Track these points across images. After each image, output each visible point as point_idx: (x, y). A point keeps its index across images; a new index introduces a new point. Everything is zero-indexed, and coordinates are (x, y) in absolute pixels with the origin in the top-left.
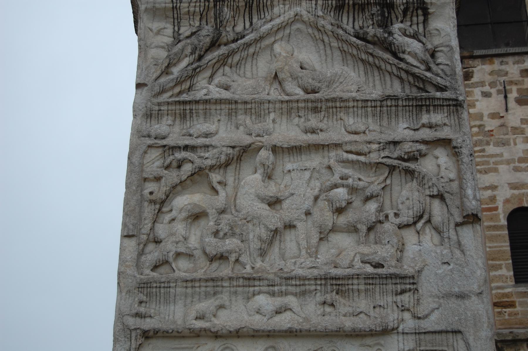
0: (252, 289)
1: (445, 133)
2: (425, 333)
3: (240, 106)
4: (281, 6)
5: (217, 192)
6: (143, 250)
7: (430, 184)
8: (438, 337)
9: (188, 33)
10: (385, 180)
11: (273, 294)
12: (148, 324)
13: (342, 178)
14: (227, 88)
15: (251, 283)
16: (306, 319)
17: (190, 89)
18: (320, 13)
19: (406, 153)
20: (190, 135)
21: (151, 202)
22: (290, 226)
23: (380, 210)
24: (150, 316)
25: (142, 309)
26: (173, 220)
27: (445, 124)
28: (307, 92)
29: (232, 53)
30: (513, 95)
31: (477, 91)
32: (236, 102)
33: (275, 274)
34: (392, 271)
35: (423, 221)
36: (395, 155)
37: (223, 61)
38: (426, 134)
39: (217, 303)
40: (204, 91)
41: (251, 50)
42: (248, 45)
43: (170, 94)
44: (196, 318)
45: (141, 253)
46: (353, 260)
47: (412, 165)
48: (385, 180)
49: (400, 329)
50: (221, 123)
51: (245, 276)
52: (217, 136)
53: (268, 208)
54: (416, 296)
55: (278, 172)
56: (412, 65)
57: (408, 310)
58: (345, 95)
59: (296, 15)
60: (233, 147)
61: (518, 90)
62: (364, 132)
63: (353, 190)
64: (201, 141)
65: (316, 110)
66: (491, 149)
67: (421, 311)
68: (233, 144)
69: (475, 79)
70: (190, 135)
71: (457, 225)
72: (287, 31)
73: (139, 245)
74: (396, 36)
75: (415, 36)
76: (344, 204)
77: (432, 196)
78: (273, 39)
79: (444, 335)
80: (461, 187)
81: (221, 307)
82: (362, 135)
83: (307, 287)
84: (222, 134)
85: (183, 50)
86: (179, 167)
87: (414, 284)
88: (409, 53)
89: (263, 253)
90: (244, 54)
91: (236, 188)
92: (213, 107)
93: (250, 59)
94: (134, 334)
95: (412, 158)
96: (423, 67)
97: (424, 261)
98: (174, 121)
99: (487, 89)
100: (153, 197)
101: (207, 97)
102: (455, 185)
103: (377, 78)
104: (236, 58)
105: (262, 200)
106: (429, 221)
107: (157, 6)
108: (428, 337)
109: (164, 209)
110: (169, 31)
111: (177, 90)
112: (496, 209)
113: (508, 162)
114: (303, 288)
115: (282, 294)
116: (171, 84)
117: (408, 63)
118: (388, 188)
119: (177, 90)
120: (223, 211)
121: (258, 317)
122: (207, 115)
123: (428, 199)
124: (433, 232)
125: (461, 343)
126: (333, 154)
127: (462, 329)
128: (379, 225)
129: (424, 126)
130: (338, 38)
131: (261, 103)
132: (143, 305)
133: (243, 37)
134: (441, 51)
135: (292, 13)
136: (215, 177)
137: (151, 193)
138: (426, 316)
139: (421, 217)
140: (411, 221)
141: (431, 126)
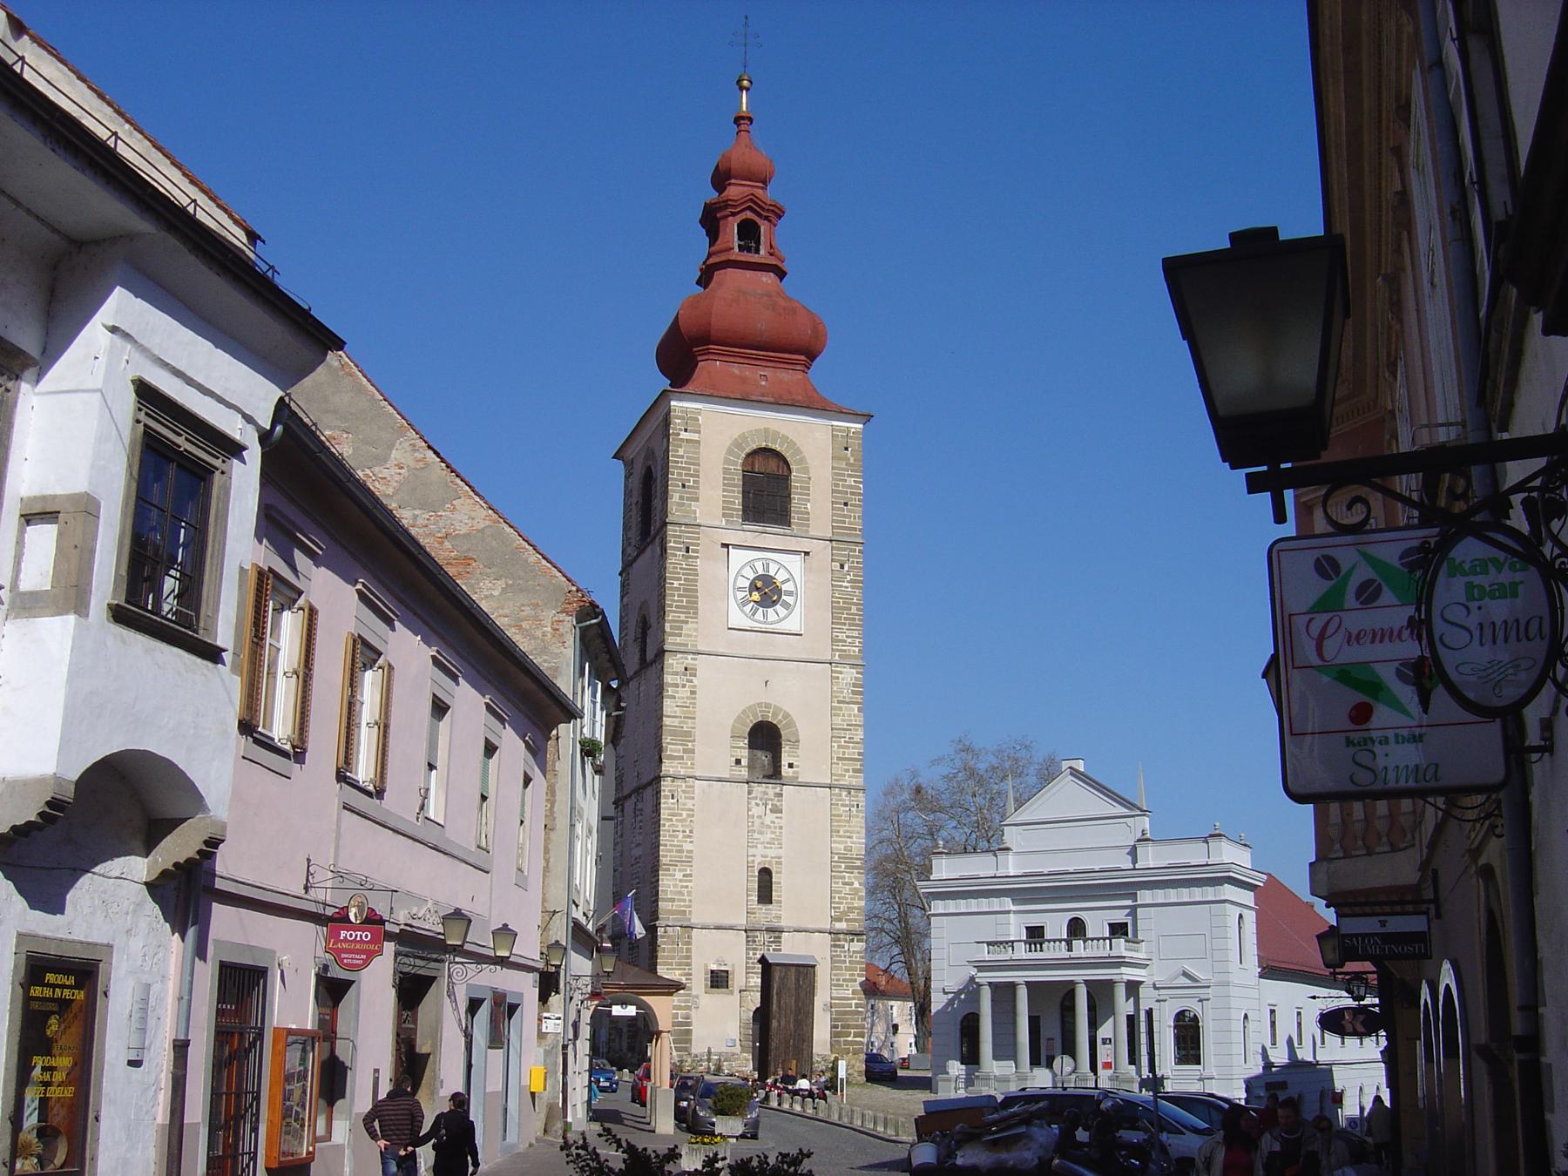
30: (769, 807)
31: (753, 802)
61: (772, 805)
66: (756, 835)
69: (753, 795)
99: (758, 801)
112: (754, 867)
113: (762, 843)
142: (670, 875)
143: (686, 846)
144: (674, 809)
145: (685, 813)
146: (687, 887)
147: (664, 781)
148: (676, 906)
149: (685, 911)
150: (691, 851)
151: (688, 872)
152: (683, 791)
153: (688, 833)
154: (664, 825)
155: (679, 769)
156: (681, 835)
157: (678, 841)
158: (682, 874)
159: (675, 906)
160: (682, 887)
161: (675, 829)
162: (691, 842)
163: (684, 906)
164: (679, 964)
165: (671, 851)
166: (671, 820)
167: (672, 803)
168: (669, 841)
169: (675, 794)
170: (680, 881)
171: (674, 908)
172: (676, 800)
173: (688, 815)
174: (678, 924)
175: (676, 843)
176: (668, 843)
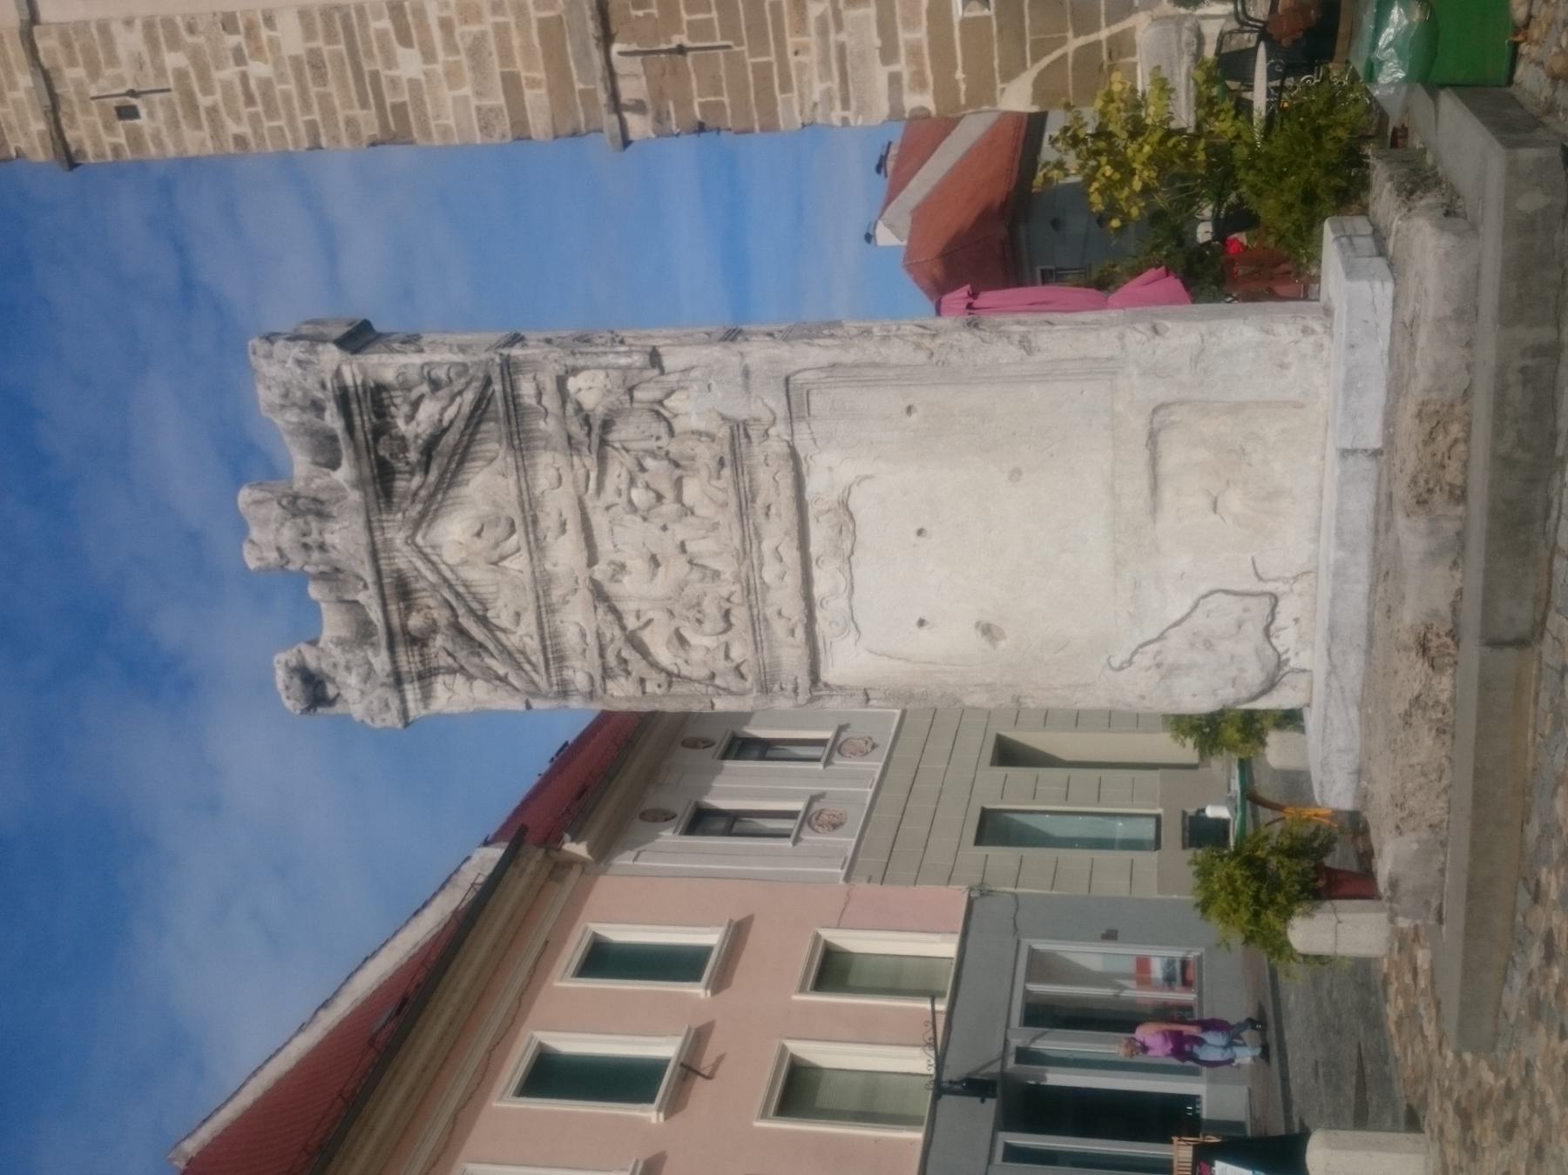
0: (758, 586)
1: (550, 386)
2: (790, 413)
3: (542, 603)
4: (397, 561)
5: (649, 622)
6: (724, 689)
7: (617, 403)
8: (793, 399)
9: (450, 660)
10: (616, 449)
11: (761, 565)
12: (804, 681)
13: (620, 495)
14: (518, 614)
15: (752, 586)
16: (787, 533)
17: (523, 653)
18: (400, 516)
19: (582, 428)
20: (584, 651)
21: (670, 686)
22: (683, 547)
23: (653, 455)
24: (796, 679)
25: (790, 687)
26: (686, 662)
27: (535, 378)
28: (512, 530)
29: (471, 611)
32: (539, 607)
33: (740, 564)
34: (727, 449)
35: (662, 411)
36: (586, 439)
37: (483, 621)
38: (550, 401)
39: (776, 617)
40: (527, 640)
41: (461, 589)
42: (457, 595)
43: (533, 674)
44: (793, 635)
45: (729, 691)
46: (718, 488)
47: (596, 424)
48: (616, 449)
49: (789, 439)
50: (564, 619)
51: (746, 593)
52: (582, 624)
53: (662, 569)
54: (752, 423)
55: (618, 558)
56: (458, 412)
57: (766, 431)
58: (514, 491)
59: (407, 543)
60: (595, 608)
62: (558, 469)
63: (632, 482)
64: (591, 640)
65: (535, 521)
67: (766, 417)
68: (592, 609)
70: (584, 651)
71: (662, 372)
72: (428, 550)
73: (719, 695)
74: (420, 430)
75: (415, 405)
76: (652, 495)
77: (632, 399)
78: (443, 567)
79: (791, 393)
80: (619, 368)
81: (780, 613)
82: (561, 471)
83: (751, 532)
84: (579, 618)
85: (477, 666)
86: (625, 661)
87: (738, 426)
88: (441, 415)
89: (716, 575)
90: (469, 598)
91: (641, 599)
92: (547, 630)
93: (473, 590)
94: (815, 694)
95: (587, 421)
96: (458, 400)
97: (709, 411)
98: (567, 667)
100: (665, 685)
101: (536, 637)
102: (613, 373)
103: (478, 448)
104: (475, 605)
105: (654, 575)
106: (661, 403)
107: (419, 696)
108: (794, 410)
109: (676, 671)
110: (448, 678)
111: (527, 667)
114: (753, 537)
115: (761, 557)
116: (523, 674)
117: (456, 416)
118: (626, 445)
119: (527, 667)
120: (671, 613)
121: (787, 579)
122: (556, 635)
123: (636, 405)
124: (673, 397)
125: (798, 376)
126: (589, 504)
127: (784, 376)
128: (671, 455)
129: (539, 402)
130: (432, 496)
131: (535, 580)
132: (784, 686)
133: (447, 601)
134: (429, 373)
135: (406, 549)
136: (631, 623)
137: (659, 686)
138: (773, 412)
139: (658, 414)
140: (663, 424)
141: (539, 394)
142: (419, 102)
143: (291, 39)
144: (169, 105)
145: (174, 60)
146: (446, 25)
147: (80, 151)
148: (529, 67)
149: (544, 24)
150: (304, 15)
151: (386, 24)
152: (94, 72)
153: (232, 40)
154: (240, 140)
155: (20, 94)
156: (259, 69)
157: (281, 77)
158: (400, 51)
159: (534, 73)
160: (451, 47)
161: (241, 99)
162: (269, 21)
163: (523, 26)
164: (759, 45)
165: (325, 99)
166: (213, 111)
167: (151, 115)
168: (291, 118)
169: (114, 102)
170: (429, 56)
171: (540, 75)
172: (133, 101)
173: (175, 43)
174: (597, 57)
175: (291, 87)
176: (301, 120)
